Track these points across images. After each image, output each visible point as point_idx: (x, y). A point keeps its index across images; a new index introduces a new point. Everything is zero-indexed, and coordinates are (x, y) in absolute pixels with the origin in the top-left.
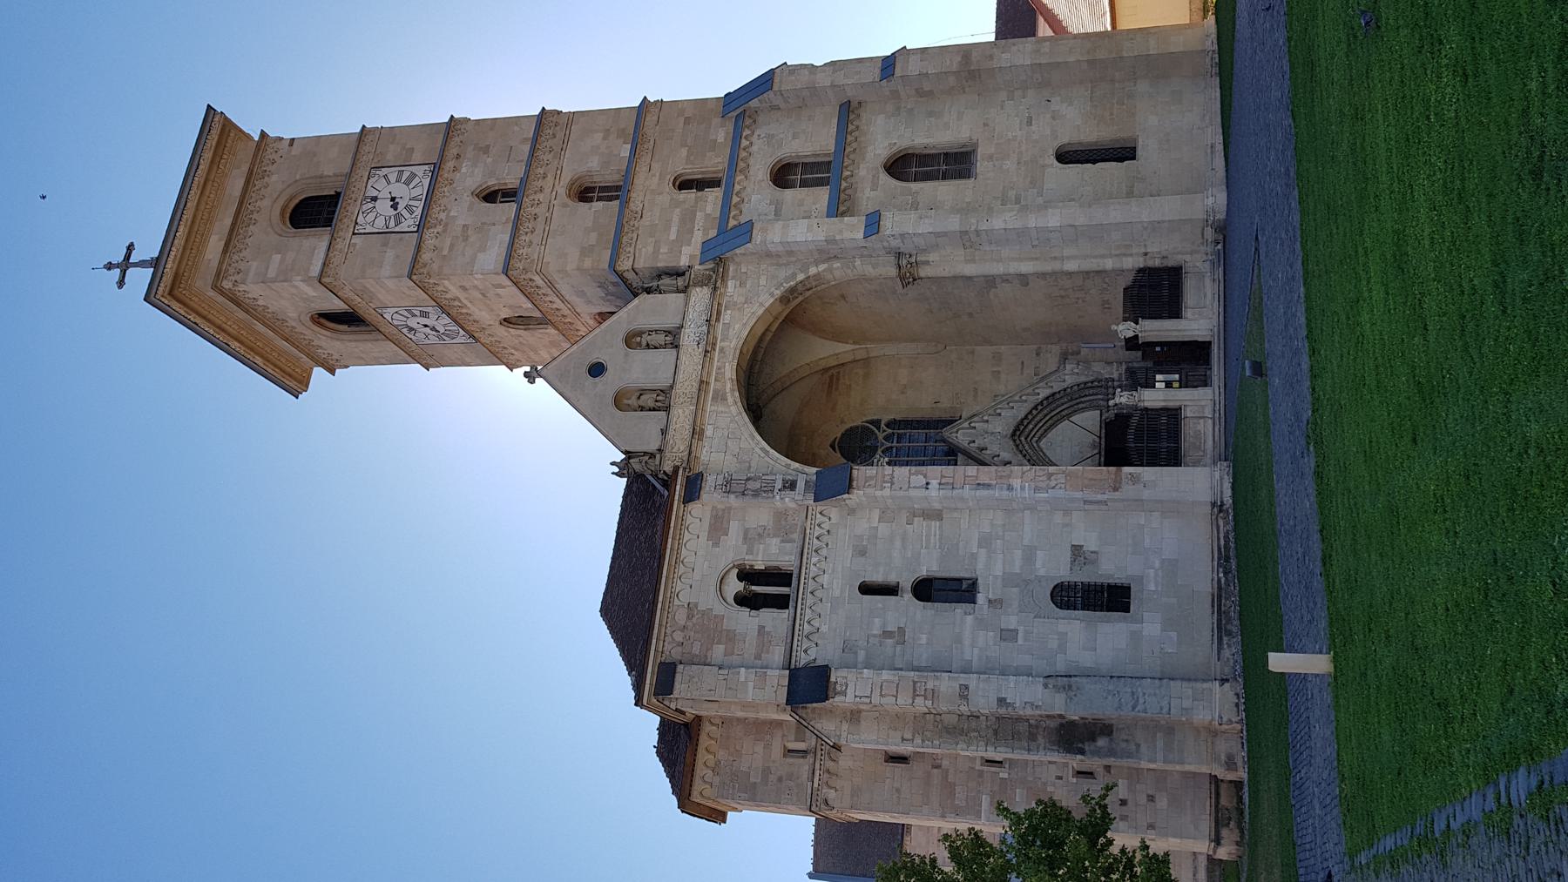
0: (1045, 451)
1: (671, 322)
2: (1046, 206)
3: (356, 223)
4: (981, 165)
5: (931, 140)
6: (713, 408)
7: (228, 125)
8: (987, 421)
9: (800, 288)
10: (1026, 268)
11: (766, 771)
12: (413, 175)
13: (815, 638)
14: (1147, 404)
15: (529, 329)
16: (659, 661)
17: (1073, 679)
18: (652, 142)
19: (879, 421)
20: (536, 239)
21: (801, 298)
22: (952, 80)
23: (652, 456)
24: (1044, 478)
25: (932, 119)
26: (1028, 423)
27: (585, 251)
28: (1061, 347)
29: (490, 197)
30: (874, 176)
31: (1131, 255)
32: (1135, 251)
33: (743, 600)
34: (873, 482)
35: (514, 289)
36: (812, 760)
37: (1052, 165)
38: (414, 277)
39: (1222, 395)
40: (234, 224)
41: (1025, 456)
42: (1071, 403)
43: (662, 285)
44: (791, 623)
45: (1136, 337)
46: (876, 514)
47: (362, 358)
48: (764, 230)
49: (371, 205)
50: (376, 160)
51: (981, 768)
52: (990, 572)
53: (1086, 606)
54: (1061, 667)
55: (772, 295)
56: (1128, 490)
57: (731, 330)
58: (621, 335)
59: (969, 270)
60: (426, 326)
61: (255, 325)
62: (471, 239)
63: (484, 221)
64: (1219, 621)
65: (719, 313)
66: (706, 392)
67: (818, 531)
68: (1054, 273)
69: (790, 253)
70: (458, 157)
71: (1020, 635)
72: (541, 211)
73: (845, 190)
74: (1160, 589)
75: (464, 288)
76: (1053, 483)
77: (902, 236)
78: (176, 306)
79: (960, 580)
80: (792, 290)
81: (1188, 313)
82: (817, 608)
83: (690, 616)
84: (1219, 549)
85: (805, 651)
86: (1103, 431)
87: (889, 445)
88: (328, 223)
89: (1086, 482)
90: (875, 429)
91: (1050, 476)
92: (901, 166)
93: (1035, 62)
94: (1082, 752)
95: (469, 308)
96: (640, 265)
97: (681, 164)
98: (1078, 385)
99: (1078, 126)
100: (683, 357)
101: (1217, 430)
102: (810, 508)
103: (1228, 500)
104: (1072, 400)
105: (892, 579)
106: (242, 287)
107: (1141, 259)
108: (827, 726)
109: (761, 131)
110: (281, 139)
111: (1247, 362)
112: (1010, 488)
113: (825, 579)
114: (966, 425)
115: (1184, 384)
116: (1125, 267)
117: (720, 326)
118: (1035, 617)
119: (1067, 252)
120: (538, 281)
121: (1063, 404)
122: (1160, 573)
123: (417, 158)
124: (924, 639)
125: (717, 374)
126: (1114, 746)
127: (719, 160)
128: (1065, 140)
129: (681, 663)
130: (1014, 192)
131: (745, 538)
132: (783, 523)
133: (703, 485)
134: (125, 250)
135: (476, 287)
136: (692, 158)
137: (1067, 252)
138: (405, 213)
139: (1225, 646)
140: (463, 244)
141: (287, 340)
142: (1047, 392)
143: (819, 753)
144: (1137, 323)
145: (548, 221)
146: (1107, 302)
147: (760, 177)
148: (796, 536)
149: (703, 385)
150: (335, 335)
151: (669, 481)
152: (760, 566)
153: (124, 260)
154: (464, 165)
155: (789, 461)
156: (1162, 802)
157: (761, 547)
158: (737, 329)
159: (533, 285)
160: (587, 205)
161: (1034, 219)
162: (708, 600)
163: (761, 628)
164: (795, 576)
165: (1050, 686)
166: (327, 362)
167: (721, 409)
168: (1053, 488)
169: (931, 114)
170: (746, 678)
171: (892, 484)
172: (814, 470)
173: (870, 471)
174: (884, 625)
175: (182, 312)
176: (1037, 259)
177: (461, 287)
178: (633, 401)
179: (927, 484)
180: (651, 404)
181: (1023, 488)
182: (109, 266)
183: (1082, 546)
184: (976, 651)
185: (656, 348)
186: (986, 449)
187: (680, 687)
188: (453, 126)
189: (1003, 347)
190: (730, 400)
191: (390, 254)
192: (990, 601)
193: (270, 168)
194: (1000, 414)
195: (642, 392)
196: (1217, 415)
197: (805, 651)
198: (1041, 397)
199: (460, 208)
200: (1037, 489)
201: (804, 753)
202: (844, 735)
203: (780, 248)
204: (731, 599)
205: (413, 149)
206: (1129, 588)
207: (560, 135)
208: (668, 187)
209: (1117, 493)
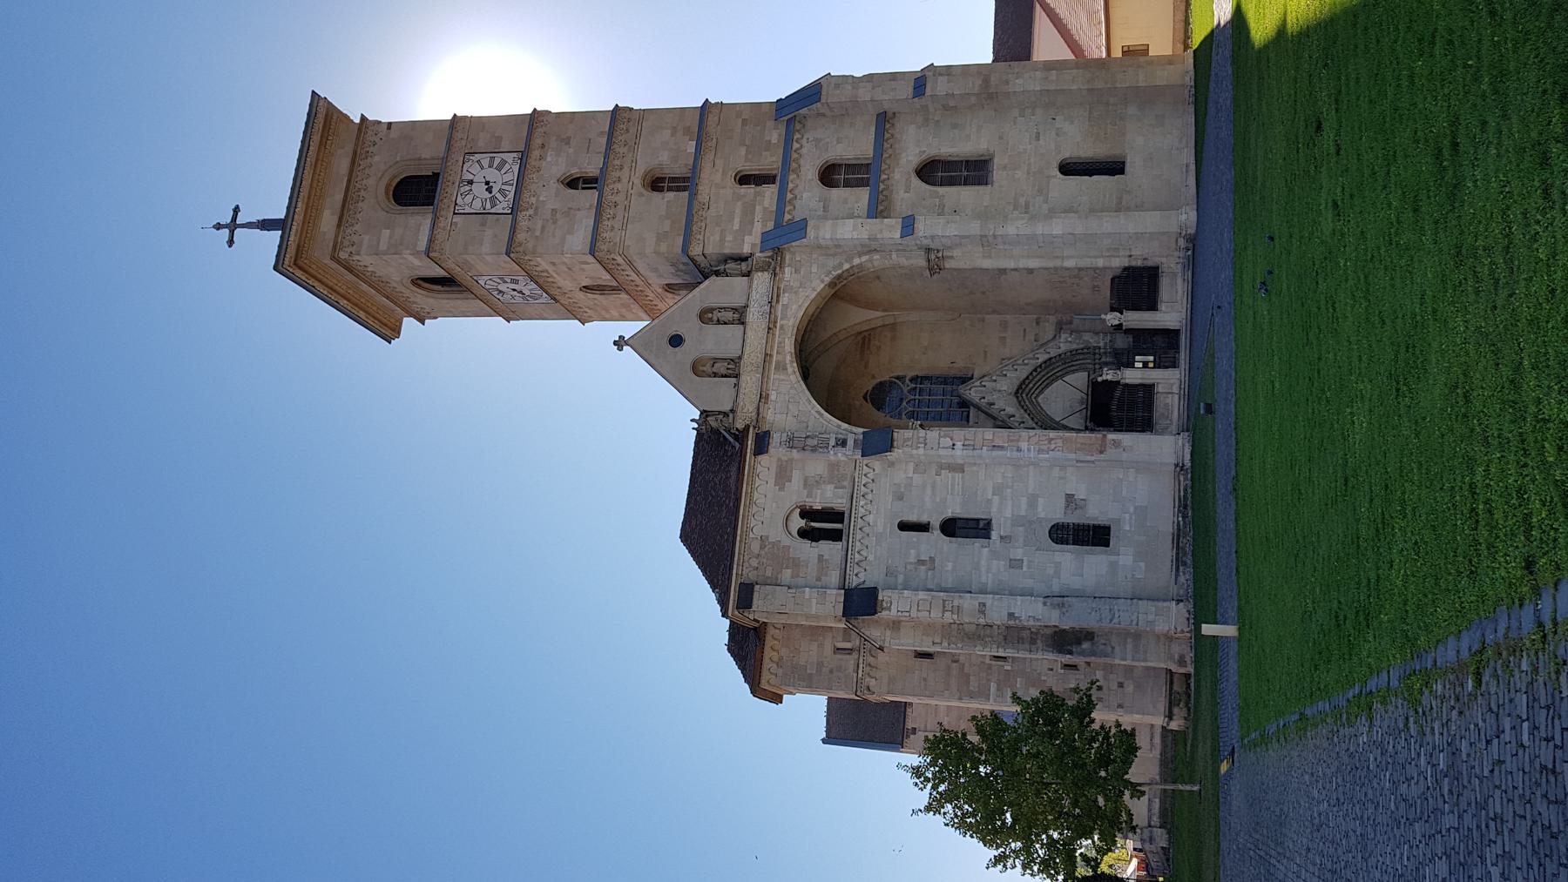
0: (1042, 405)
1: (738, 302)
2: (1052, 214)
3: (456, 204)
4: (997, 173)
6: (775, 376)
8: (995, 381)
9: (845, 275)
10: (1033, 263)
11: (820, 665)
12: (504, 162)
13: (862, 564)
14: (1127, 381)
15: (604, 294)
17: (1066, 599)
19: (904, 377)
20: (617, 225)
21: (845, 282)
22: (973, 100)
23: (726, 414)
24: (1046, 442)
25: (956, 131)
26: (1029, 383)
27: (661, 238)
28: (1057, 317)
29: (572, 183)
30: (907, 180)
31: (1119, 257)
33: (803, 534)
34: (910, 443)
35: (598, 265)
36: (856, 656)
38: (512, 255)
39: (1187, 376)
40: (345, 201)
41: (1026, 411)
42: (1064, 366)
43: (729, 269)
44: (844, 553)
45: (1121, 325)
46: (911, 467)
47: (450, 312)
48: (817, 228)
49: (467, 188)
50: (469, 146)
51: (990, 662)
52: (1003, 519)
53: (1075, 543)
54: (1056, 589)
55: (823, 281)
56: (1111, 452)
57: (789, 310)
58: (696, 311)
59: (987, 264)
60: (514, 290)
61: (360, 285)
62: (560, 223)
63: (570, 206)
64: (1177, 554)
65: (778, 296)
66: (770, 363)
71: (1025, 564)
72: (620, 198)
73: (882, 191)
74: (1133, 529)
75: (554, 264)
76: (1053, 447)
77: (933, 237)
78: (299, 273)
79: (978, 520)
80: (839, 277)
81: (1163, 307)
82: (865, 542)
83: (762, 548)
84: (1180, 499)
85: (856, 575)
86: (1090, 389)
87: (913, 397)
91: (1050, 440)
92: (931, 171)
93: (1043, 88)
94: (1071, 653)
95: (554, 278)
96: (709, 250)
98: (1071, 352)
99: (1078, 143)
100: (749, 333)
101: (1182, 403)
102: (858, 461)
103: (1188, 464)
104: (1065, 363)
105: (924, 519)
106: (356, 258)
107: (1127, 260)
108: (874, 633)
109: (810, 135)
111: (1202, 404)
112: (1019, 450)
113: (870, 518)
114: (978, 383)
115: (1157, 366)
116: (1113, 266)
118: (1036, 550)
120: (620, 260)
121: (1058, 367)
123: (505, 146)
124: (950, 566)
126: (1095, 648)
127: (774, 159)
129: (757, 584)
130: (1024, 199)
132: (836, 472)
133: (771, 441)
134: (232, 212)
135: (565, 263)
136: (750, 156)
138: (498, 195)
139: (1181, 574)
141: (388, 298)
142: (1046, 357)
143: (862, 651)
144: (1122, 313)
146: (1097, 286)
147: (810, 177)
150: (430, 294)
151: (741, 436)
152: (818, 506)
153: (232, 221)
154: (549, 154)
155: (840, 422)
156: (1130, 688)
158: (795, 309)
159: (614, 262)
161: (1041, 228)
162: (776, 533)
163: (820, 557)
164: (846, 515)
165: (1048, 604)
166: (419, 315)
167: (782, 377)
168: (1053, 450)
169: (955, 126)
170: (810, 595)
172: (861, 430)
173: (908, 434)
174: (918, 555)
175: (304, 278)
176: (1042, 257)
178: (708, 368)
179: (954, 445)
180: (723, 371)
181: (1029, 450)
182: (218, 227)
183: (1073, 495)
185: (725, 323)
186: (994, 404)
187: (757, 602)
188: (536, 119)
189: (1008, 316)
190: (790, 370)
191: (489, 232)
192: (1001, 537)
193: (371, 149)
194: (1006, 375)
195: (715, 360)
196: (1182, 392)
197: (856, 575)
199: (547, 194)
200: (1040, 451)
202: (888, 639)
203: (830, 243)
204: (795, 534)
205: (502, 138)
207: (633, 130)
208: (730, 182)
209: (1102, 455)
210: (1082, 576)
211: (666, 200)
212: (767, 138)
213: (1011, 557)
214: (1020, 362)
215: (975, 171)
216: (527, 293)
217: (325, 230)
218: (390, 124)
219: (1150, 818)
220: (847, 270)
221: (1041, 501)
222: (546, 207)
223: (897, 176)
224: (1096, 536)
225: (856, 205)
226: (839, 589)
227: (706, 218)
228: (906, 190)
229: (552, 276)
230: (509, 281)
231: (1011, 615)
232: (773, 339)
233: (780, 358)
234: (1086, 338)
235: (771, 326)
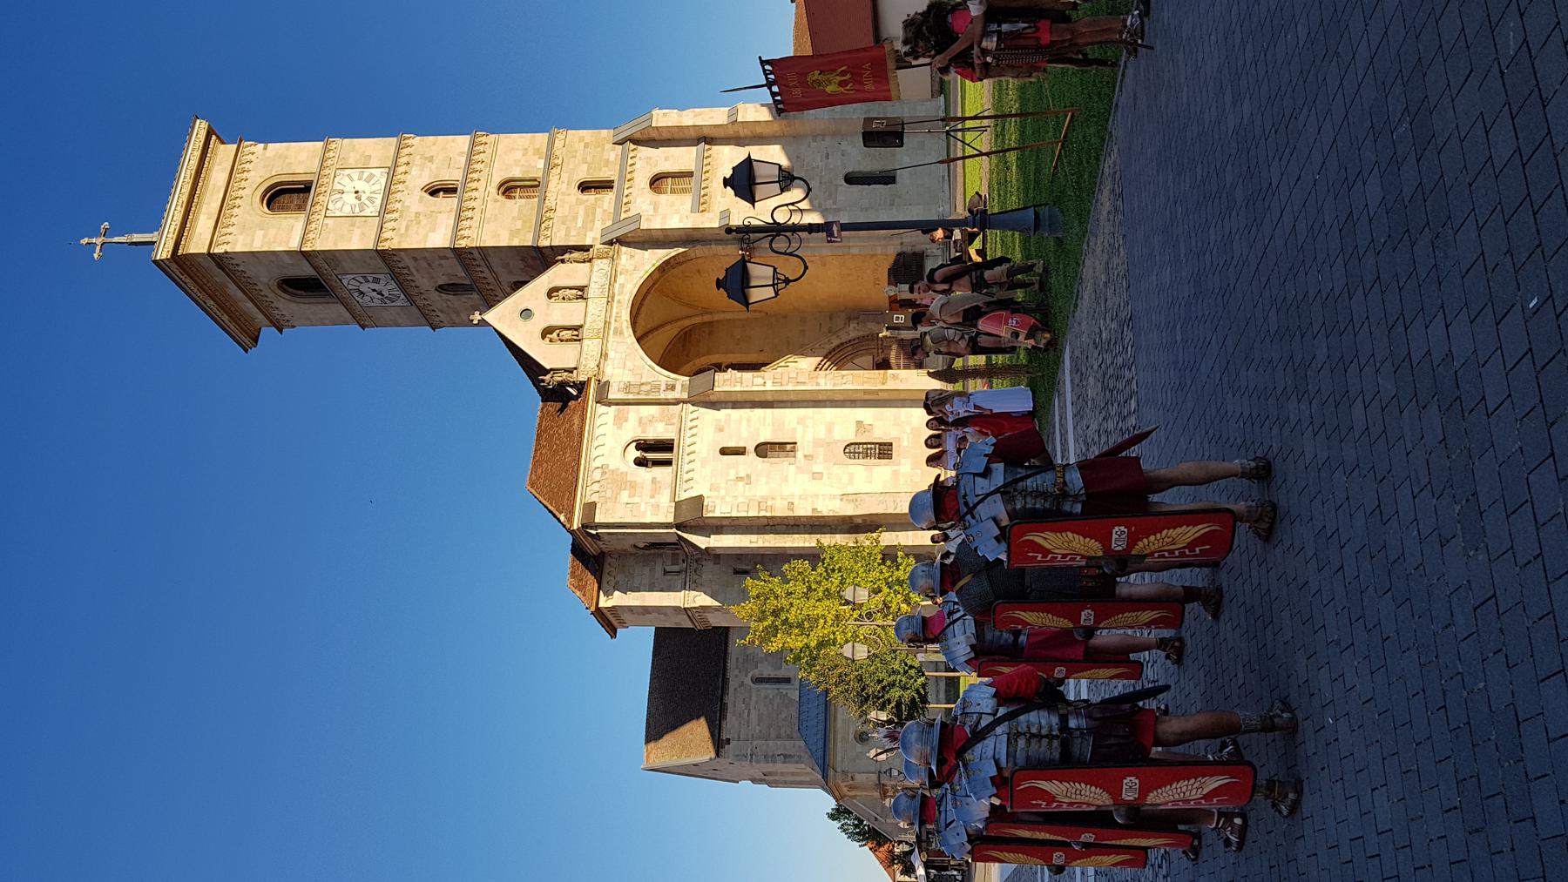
2: (839, 210)
3: (327, 209)
12: (372, 176)
18: (561, 159)
33: (640, 462)
36: (684, 576)
37: (841, 185)
47: (309, 319)
49: (339, 196)
58: (545, 290)
60: (374, 290)
62: (423, 223)
65: (616, 276)
66: (609, 329)
67: (691, 416)
75: (415, 259)
76: (844, 381)
83: (604, 473)
88: (301, 208)
89: (866, 380)
97: (584, 174)
105: (741, 444)
107: (899, 247)
112: (818, 384)
114: (783, 364)
117: (617, 286)
122: (910, 436)
127: (612, 173)
128: (851, 170)
131: (640, 423)
135: (425, 258)
136: (591, 171)
138: (367, 202)
140: (417, 226)
143: (688, 571)
147: (642, 186)
157: (652, 429)
158: (628, 287)
163: (654, 480)
167: (619, 340)
172: (688, 378)
174: (737, 473)
177: (413, 258)
181: (826, 384)
190: (626, 334)
191: (357, 232)
192: (805, 456)
198: (833, 346)
199: (412, 199)
200: (834, 385)
205: (370, 156)
212: (606, 157)
214: (817, 346)
216: (386, 294)
220: (673, 257)
222: (411, 210)
229: (412, 274)
230: (371, 279)
231: (814, 510)
233: (617, 325)
234: (870, 327)
235: (610, 300)
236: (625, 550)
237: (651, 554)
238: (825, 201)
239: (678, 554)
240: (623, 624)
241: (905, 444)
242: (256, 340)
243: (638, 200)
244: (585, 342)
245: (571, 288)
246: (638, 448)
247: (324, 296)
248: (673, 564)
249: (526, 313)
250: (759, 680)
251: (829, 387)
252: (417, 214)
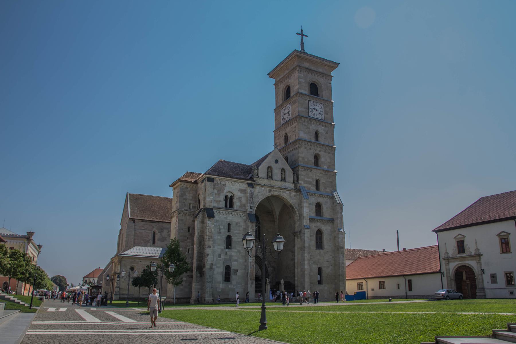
1: (287, 179)
2: (309, 265)
3: (311, 101)
5: (324, 239)
7: (334, 68)
10: (296, 260)
11: (186, 199)
15: (284, 139)
16: (214, 178)
18: (327, 174)
21: (291, 209)
22: (337, 244)
23: (257, 175)
32: (299, 284)
33: (226, 197)
34: (252, 227)
36: (188, 210)
38: (298, 116)
40: (312, 70)
44: (222, 208)
45: (281, 284)
46: (244, 227)
47: (277, 93)
48: (307, 202)
52: (233, 253)
53: (226, 273)
54: (214, 267)
55: (292, 203)
59: (296, 248)
62: (307, 130)
65: (288, 191)
66: (271, 188)
67: (241, 214)
68: (294, 266)
69: (301, 207)
70: (326, 126)
71: (220, 258)
75: (295, 127)
76: (252, 266)
77: (304, 234)
78: (293, 56)
80: (293, 208)
83: (223, 185)
90: (258, 223)
91: (253, 265)
92: (319, 234)
94: (197, 271)
95: (290, 126)
96: (300, 172)
97: (322, 181)
100: (279, 182)
105: (231, 231)
106: (297, 72)
108: (200, 216)
109: (328, 200)
110: (331, 81)
113: (231, 216)
117: (285, 191)
119: (299, 269)
120: (297, 146)
122: (232, 288)
123: (326, 116)
125: (275, 190)
127: (323, 190)
128: (323, 269)
135: (295, 130)
137: (299, 269)
144: (283, 284)
145: (310, 149)
148: (240, 209)
149: (273, 187)
151: (251, 179)
157: (238, 201)
160: (313, 158)
162: (227, 189)
163: (220, 201)
164: (231, 209)
167: (268, 191)
169: (330, 239)
171: (252, 231)
172: (254, 213)
173: (254, 226)
178: (269, 170)
181: (251, 260)
182: (302, 31)
183: (238, 272)
184: (216, 249)
187: (209, 183)
190: (269, 193)
192: (226, 252)
195: (271, 172)
197: (216, 211)
199: (314, 127)
200: (250, 262)
201: (190, 208)
202: (199, 220)
204: (227, 194)
206: (229, 281)
207: (330, 151)
210: (217, 274)
211: (312, 160)
213: (221, 255)
215: (319, 245)
217: (304, 64)
218: (331, 83)
219: (123, 294)
221: (236, 263)
223: (318, 224)
224: (227, 278)
225: (311, 213)
226: (213, 207)
227: (308, 171)
228: (315, 227)
229: (291, 126)
231: (208, 255)
232: (277, 189)
233: (273, 191)
235: (281, 189)
236: (198, 191)
237: (196, 199)
238: (313, 260)
239: (196, 208)
240: (174, 189)
241: (230, 286)
242: (271, 77)
243: (314, 199)
244: (267, 180)
245: (285, 176)
246: (231, 197)
247: (284, 98)
248: (192, 206)
249: (277, 162)
250: (154, 233)
251: (249, 260)
252: (309, 128)
